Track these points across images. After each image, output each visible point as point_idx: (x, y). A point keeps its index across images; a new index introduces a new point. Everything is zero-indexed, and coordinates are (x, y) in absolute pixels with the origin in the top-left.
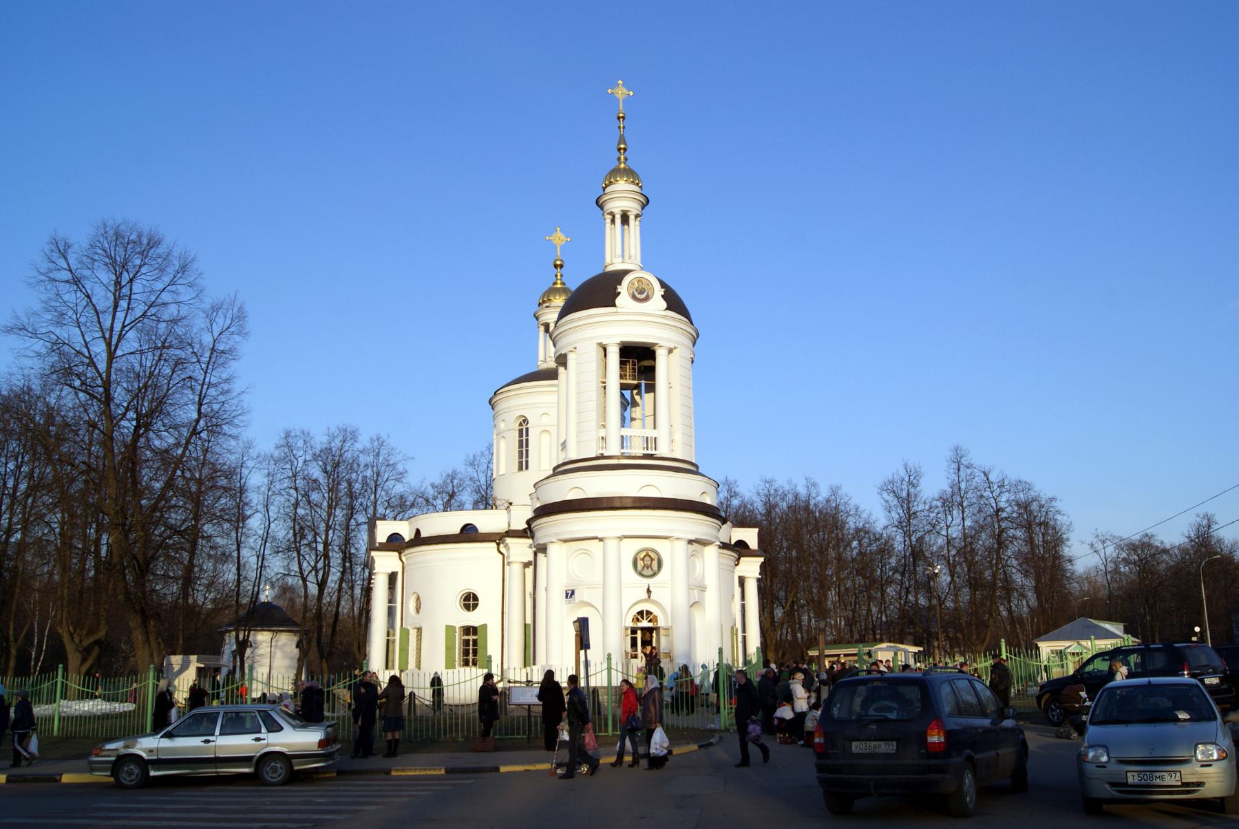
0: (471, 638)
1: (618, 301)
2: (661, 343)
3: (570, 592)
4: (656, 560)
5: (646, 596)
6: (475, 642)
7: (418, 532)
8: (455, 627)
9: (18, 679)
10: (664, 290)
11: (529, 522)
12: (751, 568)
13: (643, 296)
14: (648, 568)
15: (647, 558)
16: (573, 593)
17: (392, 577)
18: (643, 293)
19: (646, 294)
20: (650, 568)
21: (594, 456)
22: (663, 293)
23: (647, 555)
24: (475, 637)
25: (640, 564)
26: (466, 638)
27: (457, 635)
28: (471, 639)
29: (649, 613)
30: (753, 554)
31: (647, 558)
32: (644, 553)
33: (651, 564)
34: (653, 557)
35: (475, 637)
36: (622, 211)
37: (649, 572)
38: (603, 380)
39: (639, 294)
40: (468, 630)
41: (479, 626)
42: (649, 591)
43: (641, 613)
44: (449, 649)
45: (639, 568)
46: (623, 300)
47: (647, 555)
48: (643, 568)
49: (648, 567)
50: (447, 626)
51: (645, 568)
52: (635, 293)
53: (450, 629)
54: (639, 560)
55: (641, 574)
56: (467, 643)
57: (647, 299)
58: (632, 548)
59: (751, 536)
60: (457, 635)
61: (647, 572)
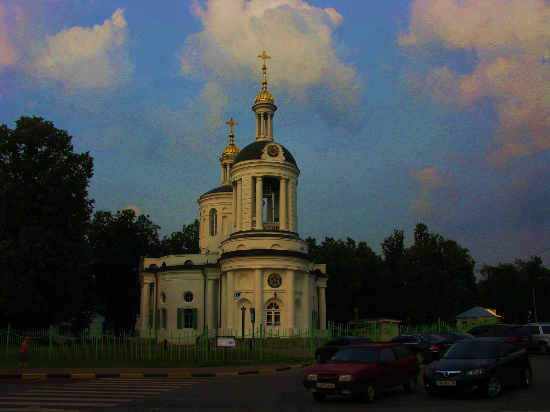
0: (190, 314)
2: (283, 177)
3: (238, 294)
4: (279, 279)
6: (191, 316)
8: (182, 309)
9: (30, 332)
10: (284, 151)
11: (218, 261)
12: (323, 283)
14: (275, 283)
16: (239, 294)
17: (152, 285)
22: (283, 153)
23: (275, 277)
24: (191, 314)
25: (271, 281)
26: (188, 314)
27: (183, 313)
28: (189, 315)
29: (275, 304)
30: (323, 276)
32: (274, 276)
34: (277, 278)
35: (191, 314)
36: (264, 113)
37: (276, 285)
38: (255, 194)
39: (272, 153)
41: (193, 309)
42: (275, 294)
43: (271, 304)
44: (179, 319)
46: (265, 156)
47: (275, 277)
48: (273, 283)
50: (178, 309)
51: (274, 283)
53: (179, 310)
54: (271, 279)
55: (272, 286)
56: (187, 317)
57: (276, 155)
59: (322, 268)
60: (183, 313)
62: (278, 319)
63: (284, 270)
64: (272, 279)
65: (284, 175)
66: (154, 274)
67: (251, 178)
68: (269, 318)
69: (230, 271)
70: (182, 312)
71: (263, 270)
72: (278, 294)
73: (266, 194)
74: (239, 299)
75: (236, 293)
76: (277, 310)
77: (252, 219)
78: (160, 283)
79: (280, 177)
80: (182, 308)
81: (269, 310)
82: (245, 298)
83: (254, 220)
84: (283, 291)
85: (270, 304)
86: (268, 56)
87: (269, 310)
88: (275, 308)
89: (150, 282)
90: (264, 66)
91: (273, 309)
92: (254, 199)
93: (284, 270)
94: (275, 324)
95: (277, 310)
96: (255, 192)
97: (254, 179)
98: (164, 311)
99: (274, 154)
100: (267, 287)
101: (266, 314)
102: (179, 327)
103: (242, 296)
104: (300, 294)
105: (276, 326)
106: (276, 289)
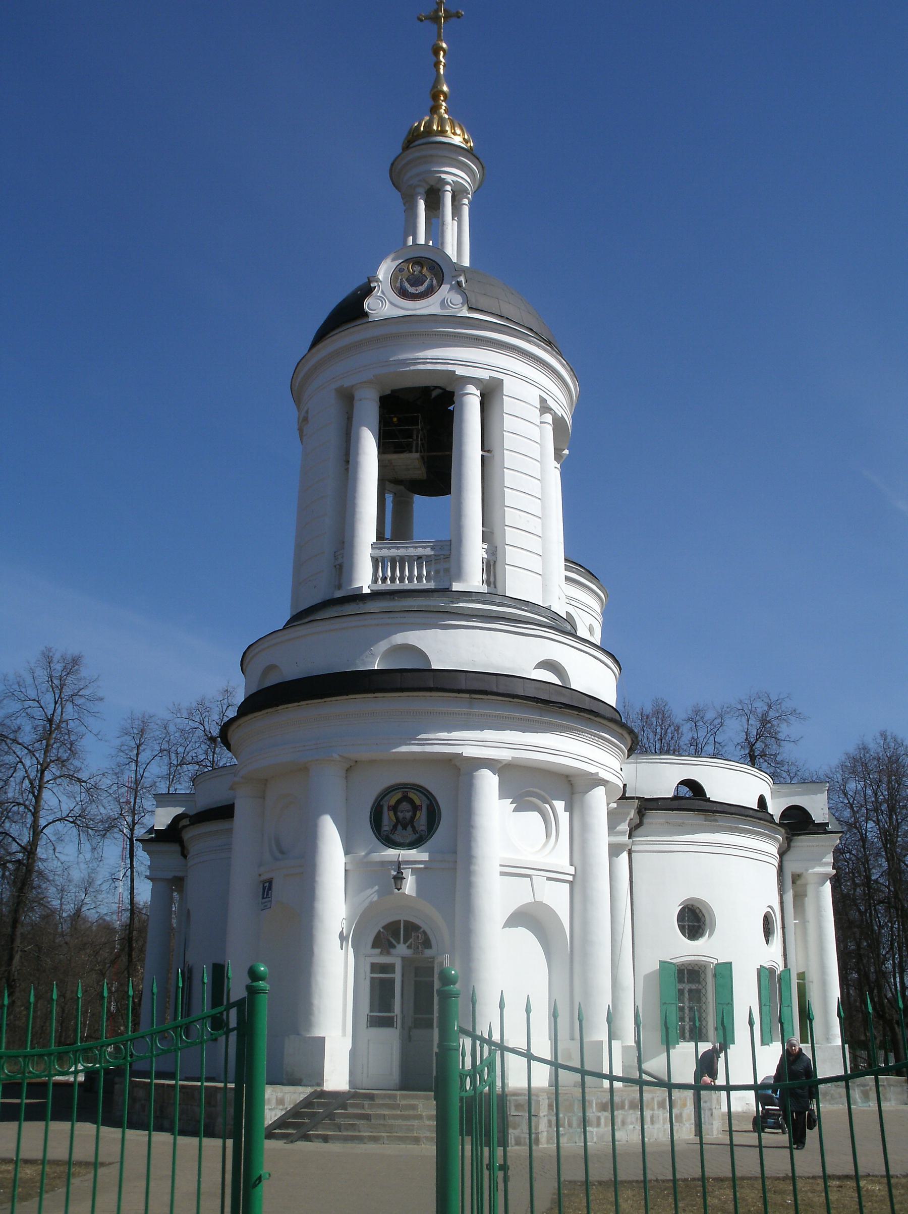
2: (460, 371)
3: (267, 884)
4: (424, 809)
13: (422, 288)
14: (405, 828)
15: (405, 805)
16: (270, 882)
19: (426, 284)
20: (409, 828)
23: (405, 798)
25: (388, 819)
31: (405, 805)
32: (398, 795)
34: (418, 802)
39: (412, 285)
45: (386, 826)
47: (405, 798)
48: (395, 827)
51: (399, 827)
52: (407, 285)
54: (385, 809)
64: (394, 808)
75: (264, 882)
99: (422, 288)
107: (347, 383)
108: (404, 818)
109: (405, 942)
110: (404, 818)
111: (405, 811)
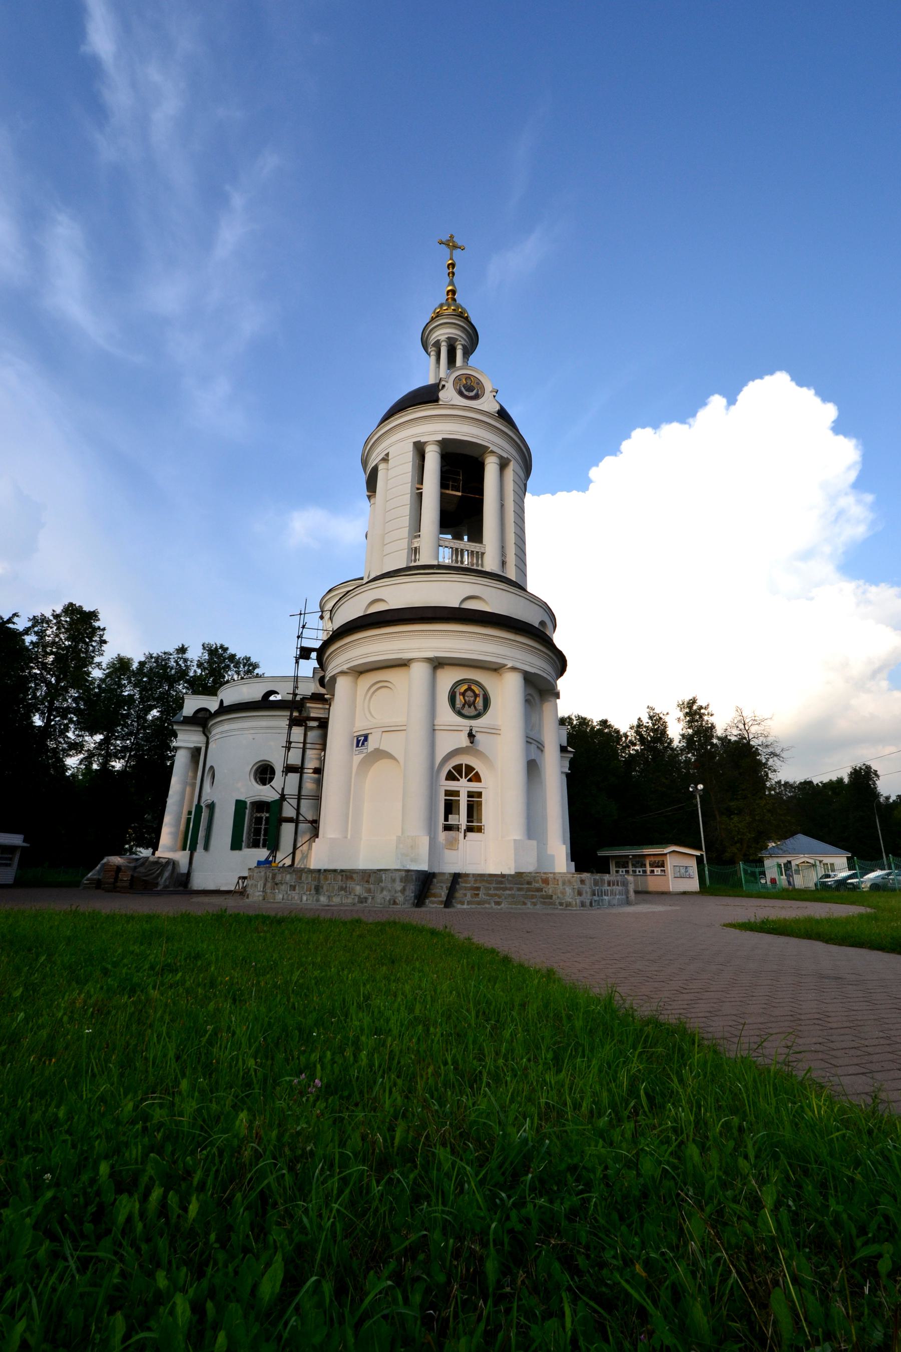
0: (265, 815)
1: (442, 395)
2: (492, 448)
3: (363, 738)
4: (481, 696)
5: (464, 742)
7: (222, 702)
8: (245, 802)
14: (470, 707)
15: (469, 693)
16: (366, 738)
17: (196, 754)
18: (472, 391)
19: (475, 392)
20: (472, 707)
21: (403, 565)
23: (469, 689)
25: (459, 700)
29: (470, 769)
31: (469, 693)
32: (465, 687)
33: (474, 701)
34: (477, 692)
35: (267, 815)
37: (471, 711)
38: (419, 486)
39: (466, 391)
40: (260, 806)
41: (272, 801)
42: (471, 736)
43: (458, 768)
47: (469, 689)
48: (464, 706)
49: (472, 704)
51: (466, 706)
53: (240, 805)
55: (460, 714)
56: (259, 821)
57: (476, 397)
58: (447, 679)
60: (247, 811)
61: (467, 711)
62: (475, 817)
63: (495, 669)
65: (494, 443)
66: (201, 729)
67: (411, 447)
68: (450, 808)
69: (342, 673)
70: (246, 808)
71: (437, 664)
72: (479, 737)
73: (448, 489)
74: (365, 751)
75: (358, 737)
76: (474, 786)
77: (410, 542)
78: (212, 746)
79: (488, 448)
80: (246, 800)
81: (452, 785)
82: (381, 748)
83: (416, 545)
84: (494, 731)
85: (454, 768)
86: (460, 244)
87: (452, 785)
88: (470, 780)
89: (192, 745)
90: (449, 285)
91: (463, 781)
92: (419, 497)
93: (495, 669)
94: (470, 829)
95: (474, 786)
96: (421, 481)
97: (420, 450)
98: (211, 807)
100: (446, 715)
101: (442, 798)
102: (236, 845)
103: (372, 744)
104: (538, 747)
105: (469, 834)
106: (473, 723)
107: (423, 440)
108: (469, 701)
109: (466, 778)
110: (469, 701)
111: (470, 696)
